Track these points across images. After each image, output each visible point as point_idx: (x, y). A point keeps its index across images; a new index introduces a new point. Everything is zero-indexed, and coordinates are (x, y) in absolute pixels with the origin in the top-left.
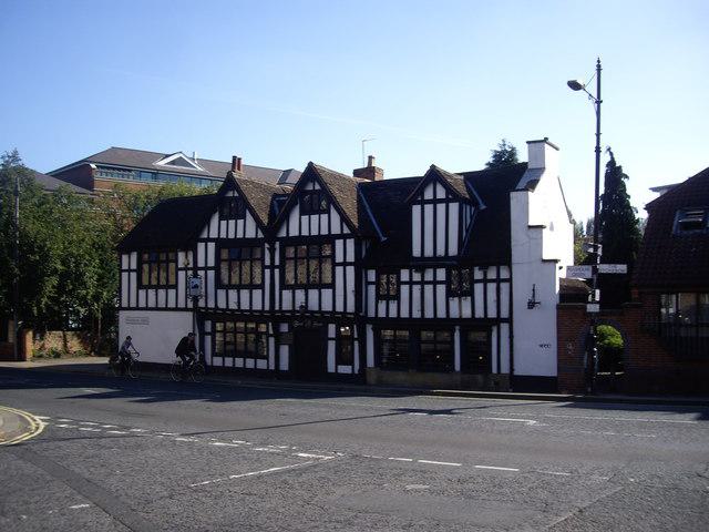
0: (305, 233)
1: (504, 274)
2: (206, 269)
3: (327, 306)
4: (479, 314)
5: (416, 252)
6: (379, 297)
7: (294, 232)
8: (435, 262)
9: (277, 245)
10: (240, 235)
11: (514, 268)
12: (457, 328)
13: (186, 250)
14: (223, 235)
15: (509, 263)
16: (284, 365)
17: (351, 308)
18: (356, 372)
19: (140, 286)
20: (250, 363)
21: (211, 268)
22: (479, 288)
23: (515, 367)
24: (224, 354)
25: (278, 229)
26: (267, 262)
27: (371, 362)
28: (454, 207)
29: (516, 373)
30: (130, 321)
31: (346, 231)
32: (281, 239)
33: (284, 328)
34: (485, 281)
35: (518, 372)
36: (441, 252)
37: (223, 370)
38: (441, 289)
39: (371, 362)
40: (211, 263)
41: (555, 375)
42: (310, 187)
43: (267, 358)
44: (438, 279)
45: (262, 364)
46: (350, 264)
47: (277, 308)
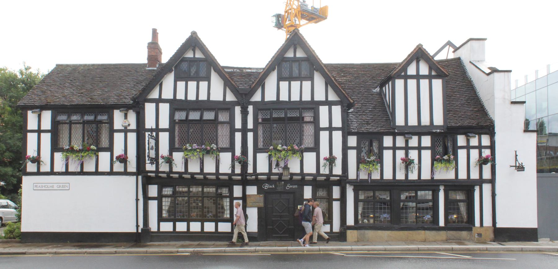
0: (284, 97)
1: (486, 140)
2: (158, 130)
3: (310, 168)
4: (462, 175)
5: (400, 121)
6: (360, 161)
7: (270, 96)
8: (420, 131)
9: (250, 109)
10: (203, 97)
11: (497, 138)
12: (442, 188)
13: (125, 108)
14: (180, 96)
16: (253, 226)
17: (338, 170)
19: (55, 147)
20: (209, 227)
21: (164, 130)
22: (462, 154)
23: (497, 221)
24: (174, 221)
25: (252, 92)
26: (238, 124)
27: (350, 221)
28: (438, 84)
29: (498, 225)
30: (36, 188)
32: (255, 104)
33: (252, 190)
34: (468, 148)
35: (500, 224)
36: (425, 121)
37: (175, 236)
38: (427, 155)
39: (350, 221)
40: (164, 123)
42: (290, 54)
44: (423, 145)
45: (224, 227)
46: (337, 129)
47: (250, 170)
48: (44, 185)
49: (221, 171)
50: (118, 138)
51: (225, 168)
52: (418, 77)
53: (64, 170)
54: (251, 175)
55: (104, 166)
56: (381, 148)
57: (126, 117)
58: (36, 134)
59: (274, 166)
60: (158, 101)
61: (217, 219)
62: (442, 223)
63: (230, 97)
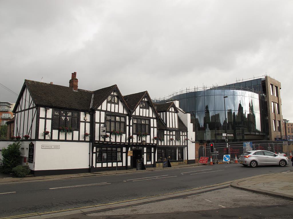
5: (168, 126)
7: (137, 114)
11: (188, 133)
13: (86, 112)
15: (187, 132)
18: (153, 163)
26: (128, 124)
27: (156, 161)
30: (43, 147)
31: (154, 116)
37: (102, 169)
39: (156, 161)
41: (194, 159)
43: (122, 161)
45: (120, 164)
47: (131, 142)
48: (47, 146)
49: (122, 142)
50: (82, 125)
51: (123, 141)
52: (172, 112)
53: (57, 139)
54: (131, 143)
55: (76, 138)
56: (164, 135)
57: (85, 116)
58: (44, 120)
59: (138, 140)
60: (101, 110)
61: (117, 162)
62: (177, 160)
63: (125, 113)
